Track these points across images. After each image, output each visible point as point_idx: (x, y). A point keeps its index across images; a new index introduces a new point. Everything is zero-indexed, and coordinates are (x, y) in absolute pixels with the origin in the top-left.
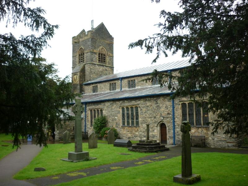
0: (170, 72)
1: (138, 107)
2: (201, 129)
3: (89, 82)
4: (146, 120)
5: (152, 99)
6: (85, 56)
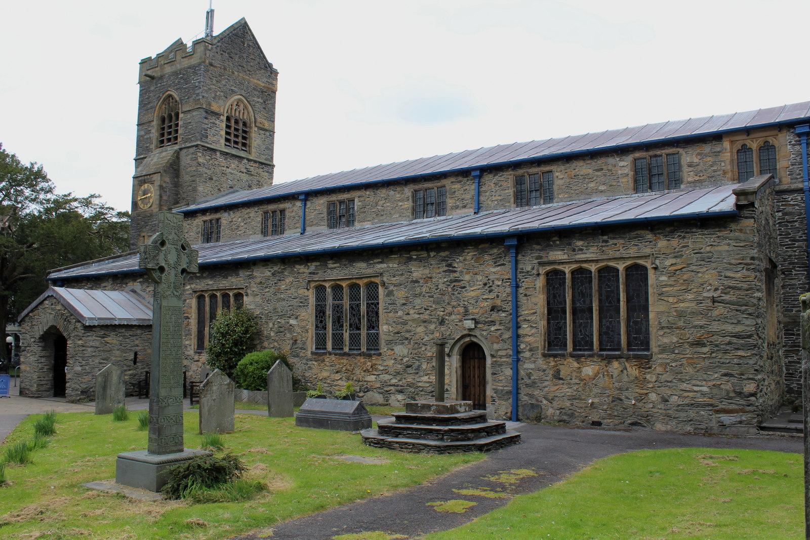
0: (478, 173)
1: (376, 286)
2: (620, 363)
3: (193, 207)
4: (409, 331)
5: (432, 254)
6: (180, 123)
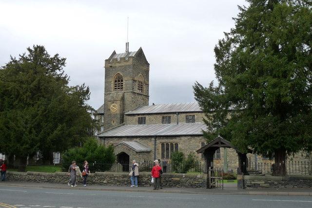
6: (124, 84)
